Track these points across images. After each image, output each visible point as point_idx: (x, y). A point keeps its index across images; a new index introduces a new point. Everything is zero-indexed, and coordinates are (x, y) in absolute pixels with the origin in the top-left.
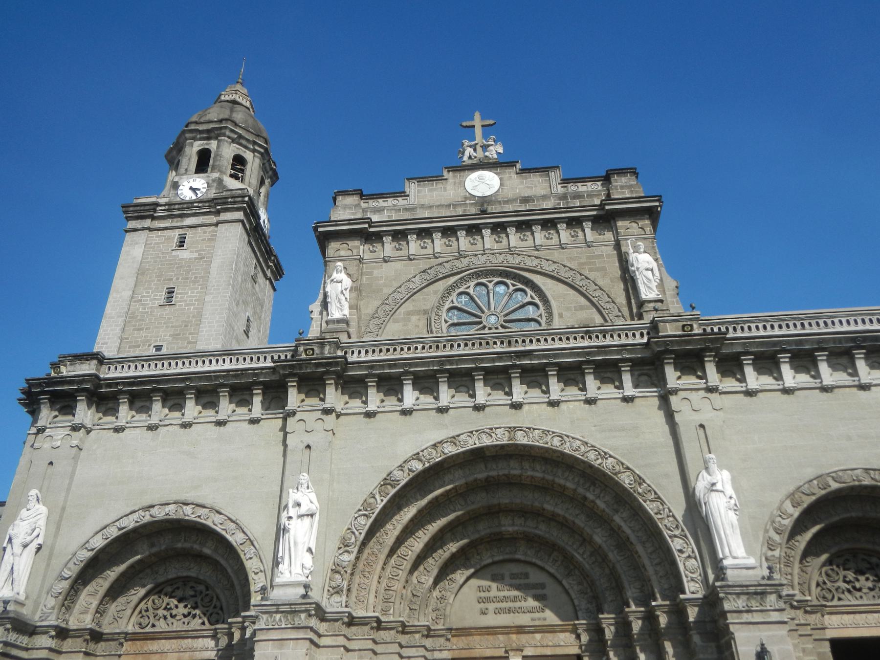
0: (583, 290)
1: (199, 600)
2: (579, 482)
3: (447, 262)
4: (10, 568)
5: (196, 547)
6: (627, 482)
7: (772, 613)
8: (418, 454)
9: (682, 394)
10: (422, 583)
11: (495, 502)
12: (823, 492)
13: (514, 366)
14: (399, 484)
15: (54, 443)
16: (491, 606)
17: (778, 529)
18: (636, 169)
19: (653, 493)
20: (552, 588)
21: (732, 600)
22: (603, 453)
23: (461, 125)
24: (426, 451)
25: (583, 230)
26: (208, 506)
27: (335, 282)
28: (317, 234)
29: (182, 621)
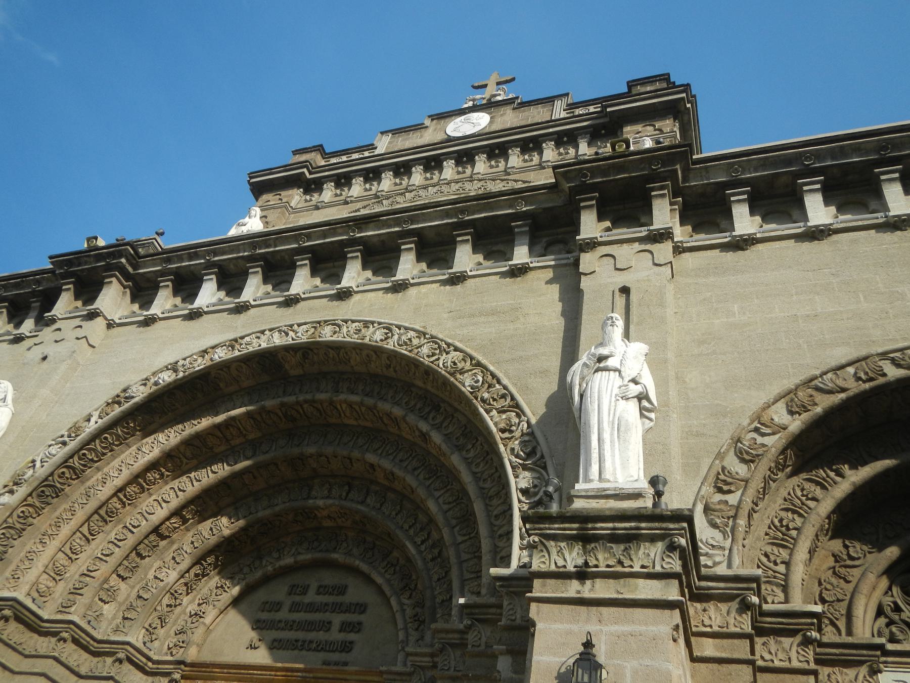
2: (415, 405)
6: (467, 384)
7: (641, 582)
8: (177, 363)
10: (159, 579)
11: (296, 451)
12: (867, 386)
13: (353, 242)
14: (129, 402)
17: (748, 453)
18: (668, 75)
19: (509, 399)
21: (554, 551)
22: (445, 346)
23: (474, 87)
24: (188, 360)
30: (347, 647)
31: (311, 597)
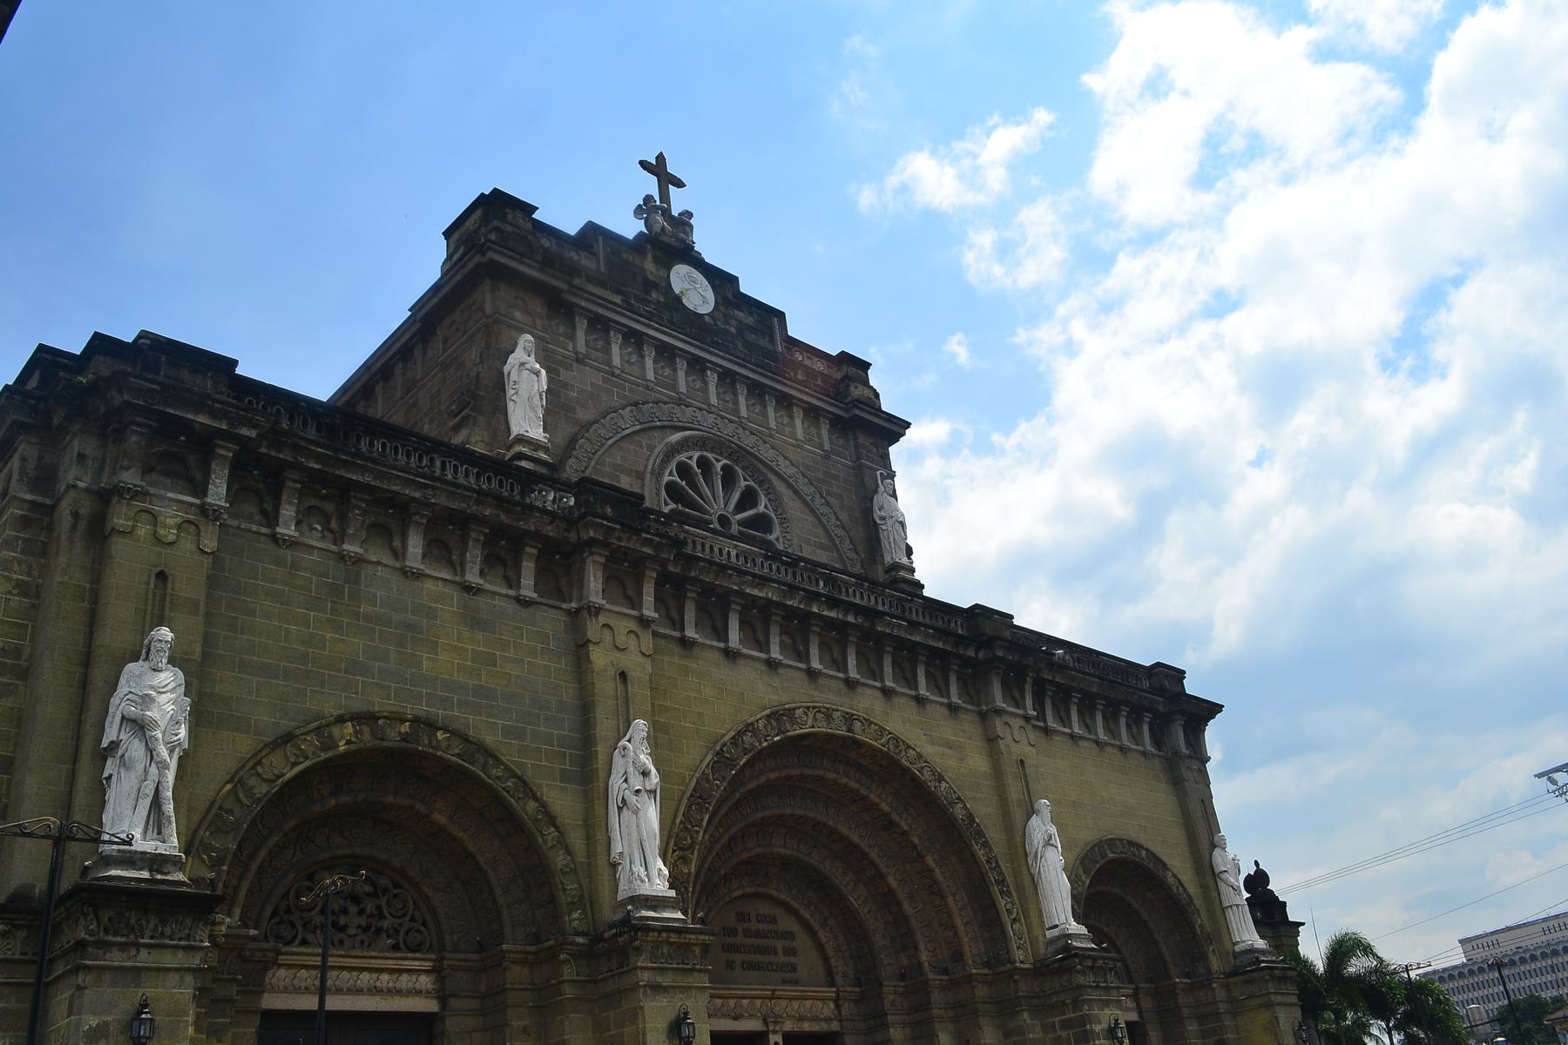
0: (824, 519)
1: (384, 905)
3: (665, 403)
4: (149, 789)
5: (422, 809)
8: (752, 724)
9: (1007, 718)
12: (1104, 861)
14: (735, 766)
15: (162, 532)
16: (739, 958)
20: (802, 941)
25: (819, 429)
26: (475, 740)
27: (527, 369)
28: (478, 258)
29: (358, 938)
30: (793, 968)
31: (754, 925)
